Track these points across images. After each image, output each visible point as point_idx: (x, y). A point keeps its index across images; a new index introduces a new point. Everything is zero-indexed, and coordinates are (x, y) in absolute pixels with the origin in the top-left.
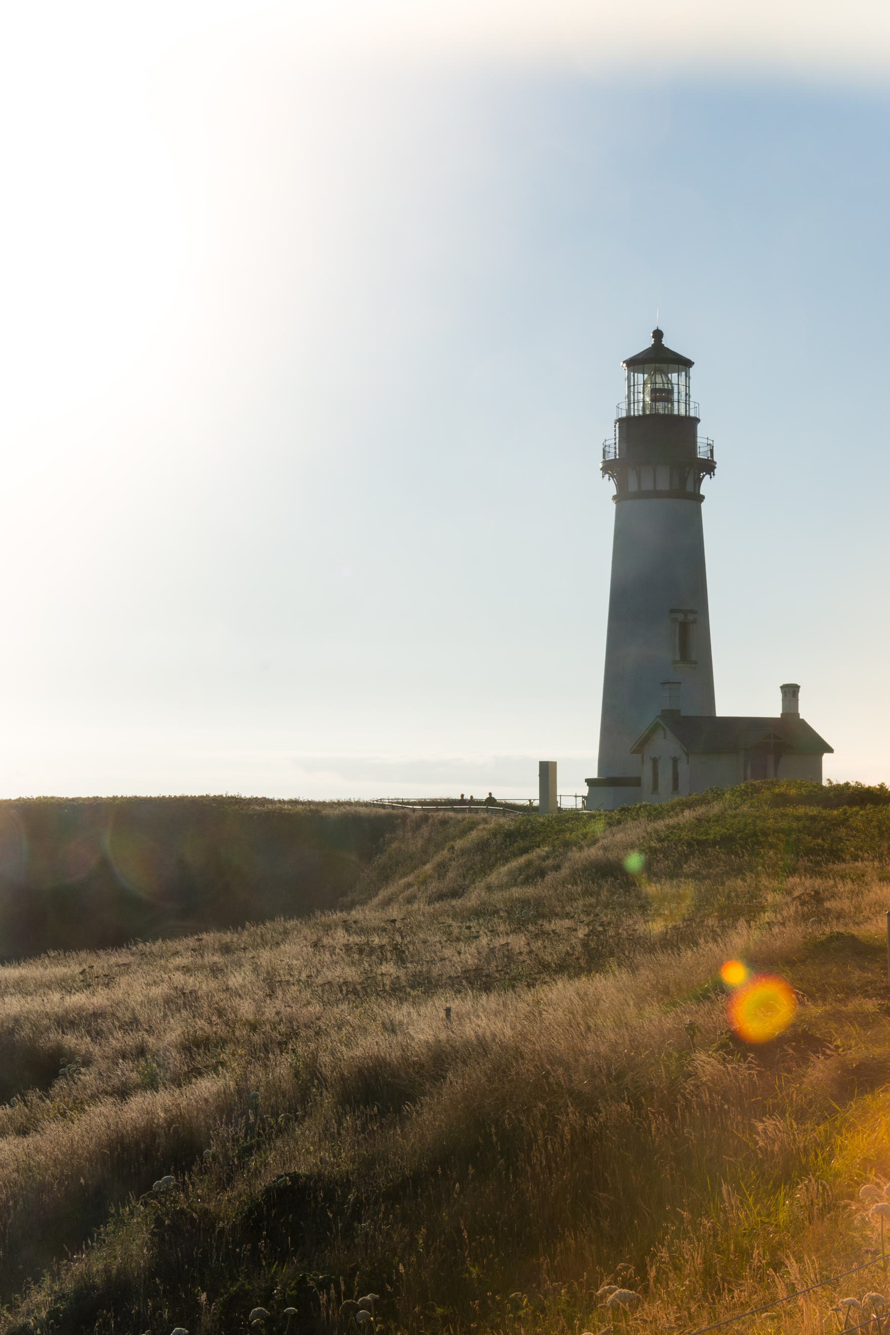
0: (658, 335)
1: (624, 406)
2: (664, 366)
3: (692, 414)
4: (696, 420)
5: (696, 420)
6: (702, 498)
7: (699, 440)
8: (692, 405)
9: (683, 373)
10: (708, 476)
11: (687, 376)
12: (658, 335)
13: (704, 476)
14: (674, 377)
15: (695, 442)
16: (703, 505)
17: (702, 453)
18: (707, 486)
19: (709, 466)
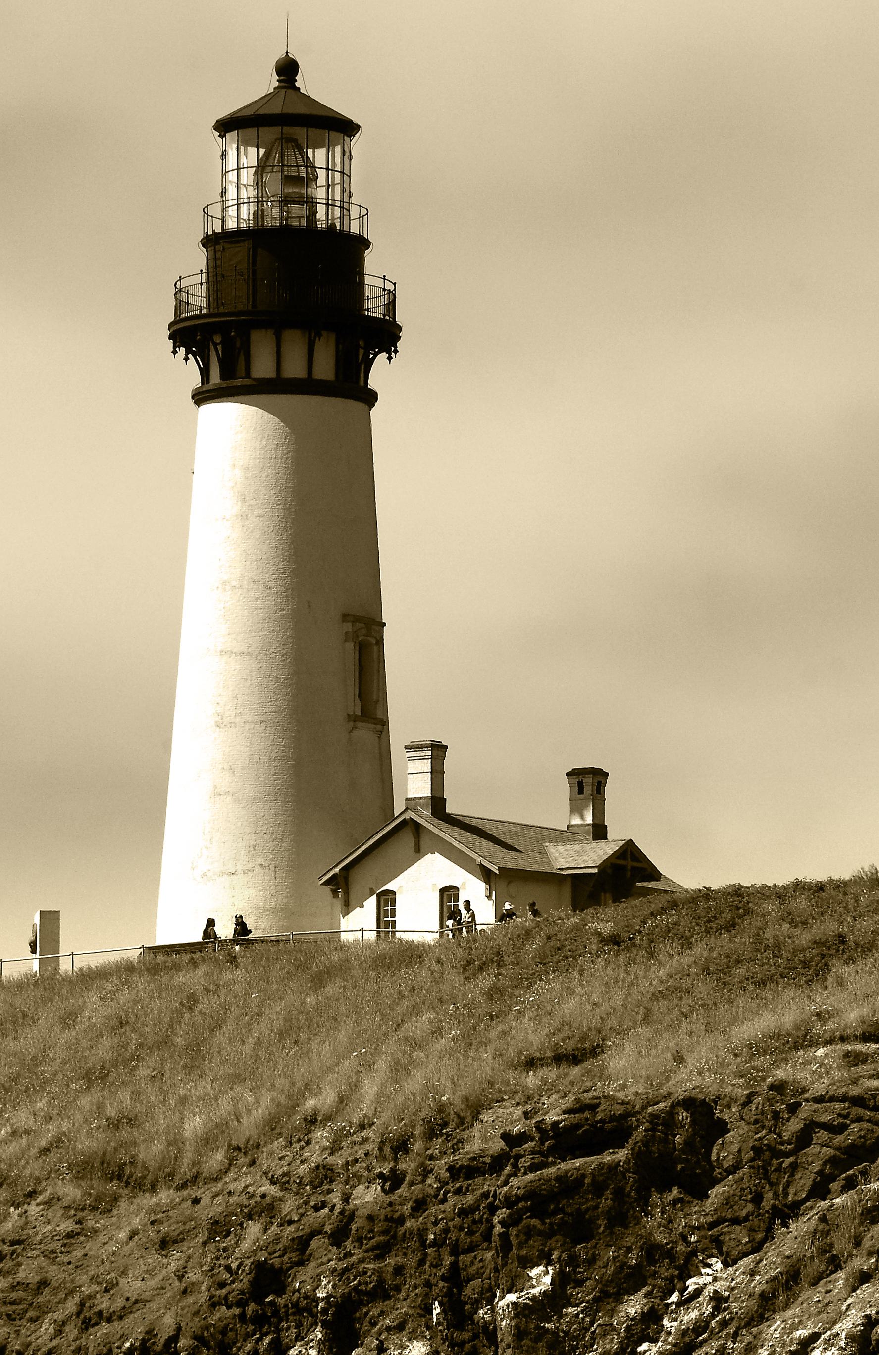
0: (288, 69)
1: (216, 210)
2: (300, 133)
3: (355, 229)
4: (366, 243)
5: (363, 243)
6: (370, 398)
7: (368, 280)
8: (355, 212)
9: (338, 149)
10: (384, 355)
11: (347, 155)
12: (288, 69)
13: (376, 355)
14: (319, 156)
15: (362, 284)
16: (376, 413)
17: (374, 307)
18: (381, 373)
19: (385, 335)
